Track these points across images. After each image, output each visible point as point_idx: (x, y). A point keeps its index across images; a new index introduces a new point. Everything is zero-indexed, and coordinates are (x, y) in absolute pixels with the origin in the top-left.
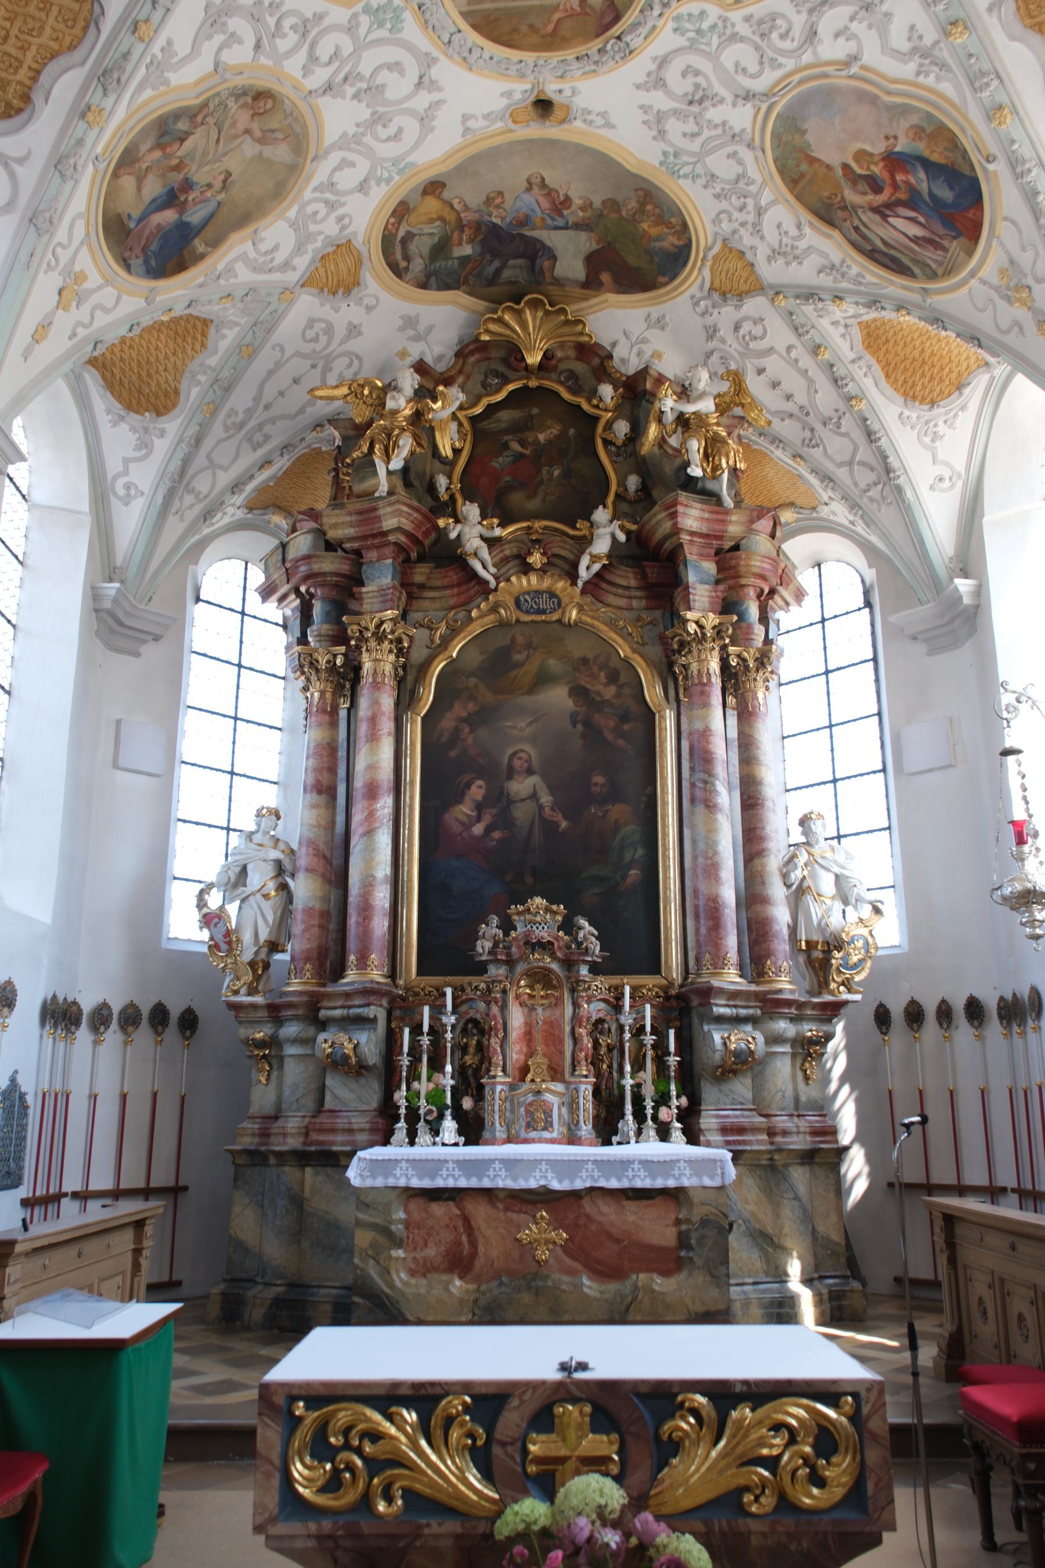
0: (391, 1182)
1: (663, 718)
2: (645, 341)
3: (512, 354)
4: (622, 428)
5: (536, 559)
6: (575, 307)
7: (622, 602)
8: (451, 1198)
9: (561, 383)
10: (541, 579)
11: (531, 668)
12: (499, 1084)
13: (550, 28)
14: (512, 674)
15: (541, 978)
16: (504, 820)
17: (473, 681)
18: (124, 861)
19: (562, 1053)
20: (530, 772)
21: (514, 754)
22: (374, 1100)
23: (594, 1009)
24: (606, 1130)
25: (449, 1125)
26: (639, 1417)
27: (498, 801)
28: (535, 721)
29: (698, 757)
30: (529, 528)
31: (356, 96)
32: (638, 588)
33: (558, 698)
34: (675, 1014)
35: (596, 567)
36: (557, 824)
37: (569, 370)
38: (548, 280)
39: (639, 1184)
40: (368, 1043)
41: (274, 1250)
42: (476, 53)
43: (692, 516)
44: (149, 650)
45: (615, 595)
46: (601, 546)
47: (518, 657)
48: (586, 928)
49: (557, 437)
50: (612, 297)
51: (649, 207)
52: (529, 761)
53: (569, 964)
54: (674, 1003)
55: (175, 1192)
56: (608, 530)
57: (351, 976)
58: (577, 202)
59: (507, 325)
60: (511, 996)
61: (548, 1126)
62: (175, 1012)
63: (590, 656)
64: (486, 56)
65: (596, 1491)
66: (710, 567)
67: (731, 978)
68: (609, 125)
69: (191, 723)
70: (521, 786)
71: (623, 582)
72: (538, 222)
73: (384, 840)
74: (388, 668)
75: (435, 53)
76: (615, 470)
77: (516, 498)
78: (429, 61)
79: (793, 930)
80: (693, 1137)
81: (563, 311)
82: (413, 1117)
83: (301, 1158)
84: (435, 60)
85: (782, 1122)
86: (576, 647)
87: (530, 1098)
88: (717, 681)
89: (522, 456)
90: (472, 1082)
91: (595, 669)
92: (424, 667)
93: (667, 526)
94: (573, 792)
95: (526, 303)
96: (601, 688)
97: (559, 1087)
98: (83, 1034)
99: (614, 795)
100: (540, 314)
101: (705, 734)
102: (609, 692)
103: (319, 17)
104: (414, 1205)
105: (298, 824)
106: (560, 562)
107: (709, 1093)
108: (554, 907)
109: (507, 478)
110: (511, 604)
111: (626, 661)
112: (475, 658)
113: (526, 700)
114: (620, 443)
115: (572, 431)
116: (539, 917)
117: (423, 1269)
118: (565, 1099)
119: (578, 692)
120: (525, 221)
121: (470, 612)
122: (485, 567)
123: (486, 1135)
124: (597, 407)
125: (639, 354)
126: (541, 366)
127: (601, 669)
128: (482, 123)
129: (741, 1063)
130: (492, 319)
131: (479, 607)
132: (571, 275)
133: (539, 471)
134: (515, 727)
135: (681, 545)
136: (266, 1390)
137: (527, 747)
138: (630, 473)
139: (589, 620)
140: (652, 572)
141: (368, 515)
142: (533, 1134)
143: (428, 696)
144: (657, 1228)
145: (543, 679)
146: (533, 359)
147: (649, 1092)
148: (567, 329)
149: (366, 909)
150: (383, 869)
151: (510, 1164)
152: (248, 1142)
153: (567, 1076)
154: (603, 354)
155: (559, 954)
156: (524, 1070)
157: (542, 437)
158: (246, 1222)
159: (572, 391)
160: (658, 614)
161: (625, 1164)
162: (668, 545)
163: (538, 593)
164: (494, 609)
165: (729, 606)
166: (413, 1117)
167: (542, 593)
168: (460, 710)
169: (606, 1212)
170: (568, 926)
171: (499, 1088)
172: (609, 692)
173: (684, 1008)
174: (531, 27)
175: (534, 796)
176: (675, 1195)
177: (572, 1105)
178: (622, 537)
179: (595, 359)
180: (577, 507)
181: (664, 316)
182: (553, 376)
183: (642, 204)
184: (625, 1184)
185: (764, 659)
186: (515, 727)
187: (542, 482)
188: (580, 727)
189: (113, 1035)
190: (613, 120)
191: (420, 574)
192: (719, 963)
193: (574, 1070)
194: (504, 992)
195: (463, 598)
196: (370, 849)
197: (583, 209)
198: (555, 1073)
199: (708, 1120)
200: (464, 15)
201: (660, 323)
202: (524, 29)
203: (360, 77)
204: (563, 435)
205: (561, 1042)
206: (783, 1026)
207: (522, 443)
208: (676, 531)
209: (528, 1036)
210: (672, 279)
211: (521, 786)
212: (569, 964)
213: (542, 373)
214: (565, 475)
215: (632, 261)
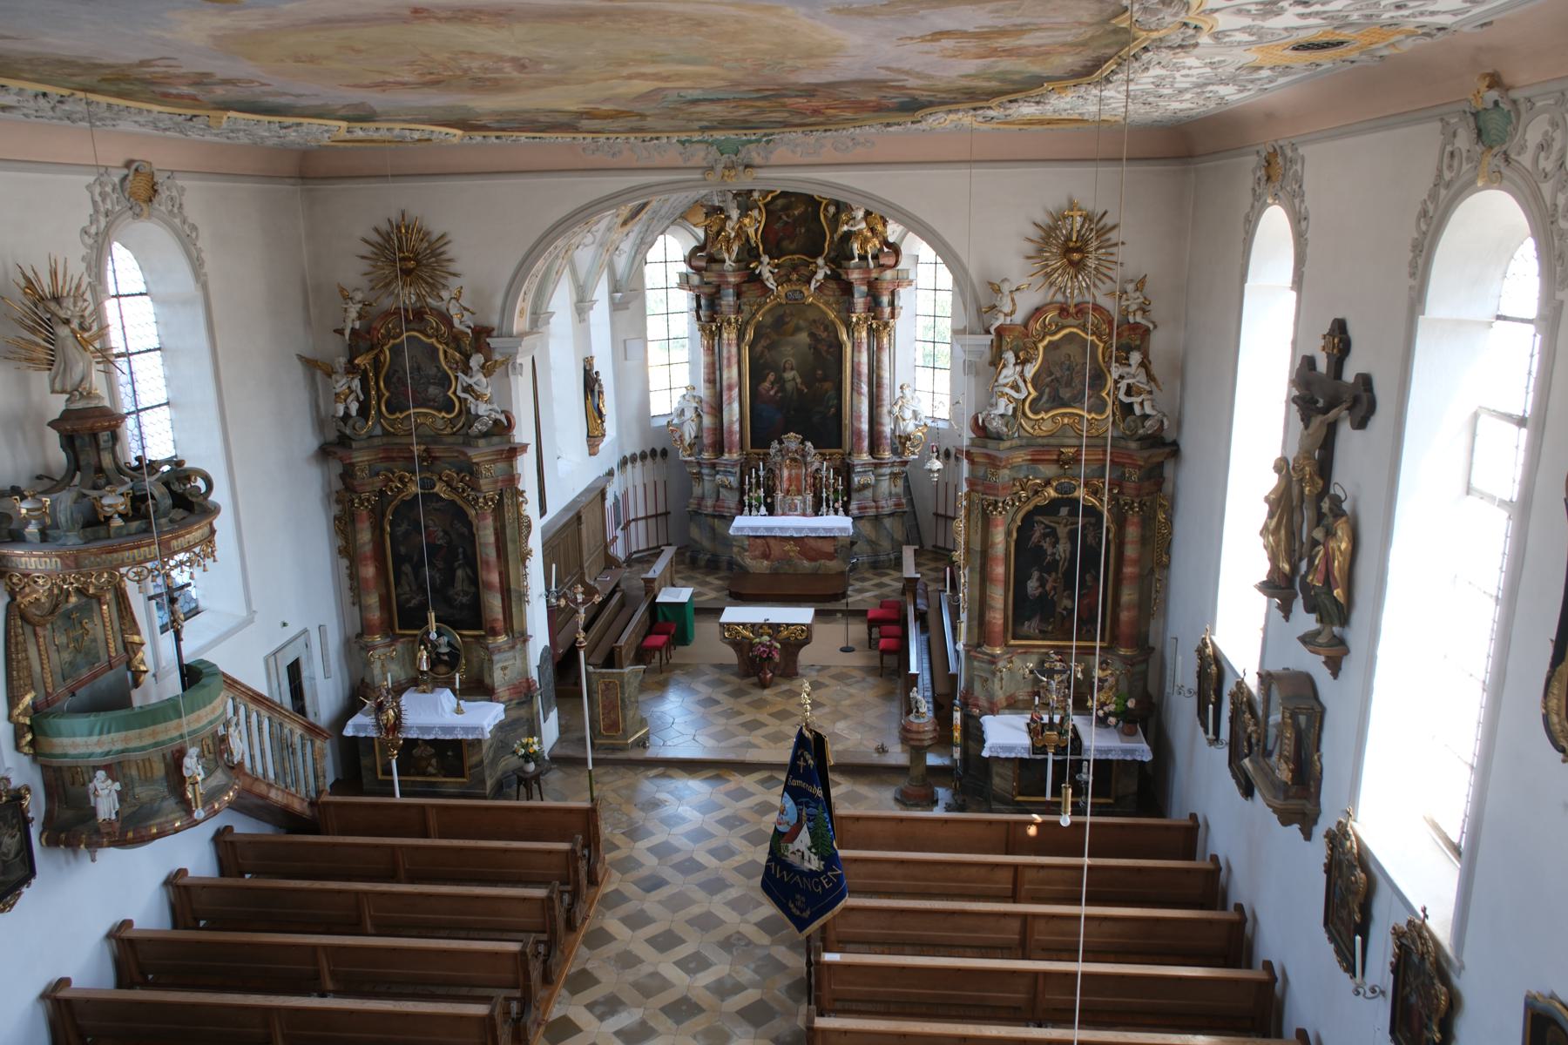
5: (795, 277)
11: (792, 324)
12: (780, 495)
15: (794, 460)
16: (782, 389)
18: (634, 397)
22: (737, 498)
23: (816, 465)
24: (816, 513)
25: (763, 510)
26: (775, 627)
27: (780, 380)
29: (856, 372)
33: (803, 337)
40: (733, 481)
41: (706, 543)
43: (855, 276)
44: (633, 306)
46: (820, 275)
48: (809, 444)
53: (803, 456)
55: (667, 514)
57: (726, 456)
62: (659, 451)
65: (766, 638)
66: (864, 288)
67: (865, 457)
69: (650, 321)
70: (789, 375)
73: (736, 406)
74: (733, 336)
79: (893, 431)
80: (847, 513)
82: (750, 506)
83: (714, 516)
85: (883, 503)
86: (811, 315)
88: (865, 341)
89: (786, 223)
90: (770, 492)
92: (747, 323)
94: (808, 377)
98: (629, 466)
99: (825, 379)
101: (859, 363)
102: (824, 335)
105: (703, 391)
107: (855, 496)
111: (833, 323)
112: (769, 320)
116: (792, 440)
117: (755, 558)
119: (812, 335)
129: (865, 487)
136: (722, 625)
141: (722, 275)
143: (750, 335)
144: (828, 547)
145: (798, 329)
147: (832, 497)
149: (731, 432)
150: (736, 416)
151: (781, 529)
152: (692, 507)
158: (695, 533)
165: (874, 305)
166: (750, 506)
168: (763, 343)
169: (812, 543)
170: (802, 443)
172: (824, 335)
173: (845, 470)
176: (834, 538)
185: (886, 325)
189: (639, 463)
191: (744, 288)
192: (860, 452)
196: (731, 410)
198: (799, 492)
199: (853, 506)
206: (887, 470)
209: (790, 478)
211: (789, 375)
212: (803, 456)
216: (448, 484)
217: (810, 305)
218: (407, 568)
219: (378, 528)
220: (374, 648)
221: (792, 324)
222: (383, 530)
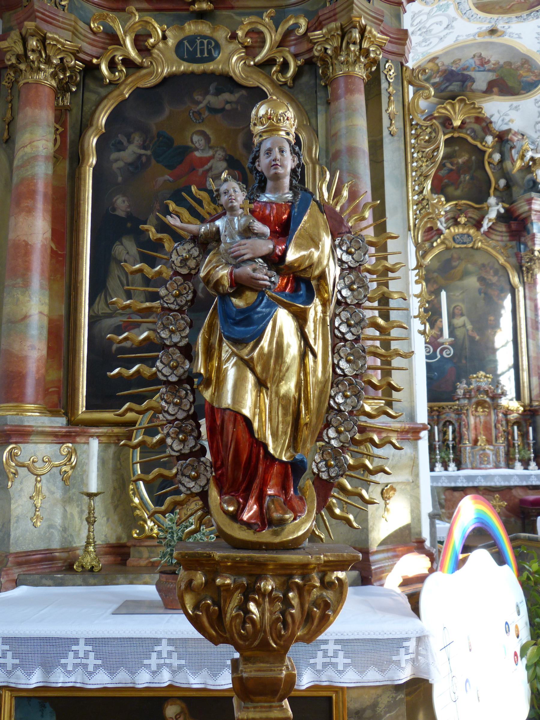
0: (440, 485)
1: (518, 291)
2: (507, 115)
3: (446, 122)
4: (497, 157)
5: (462, 220)
6: (478, 100)
7: (499, 238)
8: (462, 490)
9: (468, 135)
10: (464, 229)
11: (461, 268)
13: (508, 7)
14: (453, 271)
17: (435, 274)
19: (491, 434)
20: (462, 315)
21: (455, 307)
28: (463, 292)
30: (456, 204)
31: (420, 35)
32: (507, 232)
33: (472, 282)
34: (528, 417)
35: (490, 224)
36: (474, 338)
37: (471, 128)
38: (468, 89)
39: (534, 483)
42: (475, 16)
45: (496, 235)
46: (493, 215)
47: (455, 264)
49: (467, 161)
50: (496, 97)
51: (526, 66)
52: (461, 310)
54: (529, 413)
56: (497, 208)
58: (493, 61)
59: (447, 110)
60: (470, 412)
61: (489, 463)
63: (486, 263)
64: (478, 17)
68: (520, 38)
71: (500, 229)
72: (472, 69)
75: (457, 16)
76: (494, 177)
77: (450, 190)
78: (454, 19)
81: (474, 103)
84: (456, 19)
86: (480, 259)
87: (481, 452)
89: (451, 170)
91: (488, 269)
93: (527, 208)
95: (458, 101)
96: (491, 278)
97: (491, 447)
100: (462, 105)
102: (494, 279)
103: (420, 12)
104: (447, 493)
106: (472, 220)
108: (488, 375)
109: (446, 181)
110: (451, 240)
112: (436, 265)
113: (459, 283)
114: (495, 164)
115: (473, 158)
118: (494, 452)
119: (482, 280)
120: (466, 69)
121: (432, 243)
122: (441, 224)
123: (463, 466)
124: (484, 146)
125: (503, 120)
126: (460, 127)
127: (490, 269)
128: (465, 37)
130: (441, 108)
131: (436, 241)
132: (479, 88)
133: (459, 177)
134: (454, 295)
135: (530, 216)
137: (460, 304)
138: (502, 178)
139: (486, 247)
140: (514, 226)
142: (483, 466)
145: (466, 274)
146: (457, 123)
148: (473, 111)
153: (494, 443)
154: (488, 121)
155: (491, 395)
156: (476, 441)
157: (460, 161)
159: (474, 139)
160: (514, 243)
161: (529, 476)
162: (524, 216)
163: (462, 235)
164: (443, 243)
167: (464, 234)
171: (468, 448)
172: (494, 279)
174: (501, 7)
175: (464, 326)
177: (497, 454)
178: (502, 211)
179: (484, 124)
180: (480, 196)
181: (519, 106)
182: (464, 131)
183: (523, 65)
184: (529, 483)
186: (454, 295)
187: (461, 182)
188: (483, 295)
190: (522, 36)
193: (496, 440)
194: (467, 410)
195: (429, 237)
197: (494, 64)
198: (489, 442)
200: (474, 4)
201: (517, 108)
202: (497, 7)
203: (424, 27)
204: (469, 160)
205: (491, 429)
207: (452, 164)
208: (530, 210)
209: (476, 428)
210: (527, 92)
213: (460, 130)
214: (472, 178)
215: (510, 84)
216: (250, 51)
217: (478, 249)
218: (126, 249)
219: (69, 153)
220: (22, 434)
221: (461, 268)
222: (77, 159)
